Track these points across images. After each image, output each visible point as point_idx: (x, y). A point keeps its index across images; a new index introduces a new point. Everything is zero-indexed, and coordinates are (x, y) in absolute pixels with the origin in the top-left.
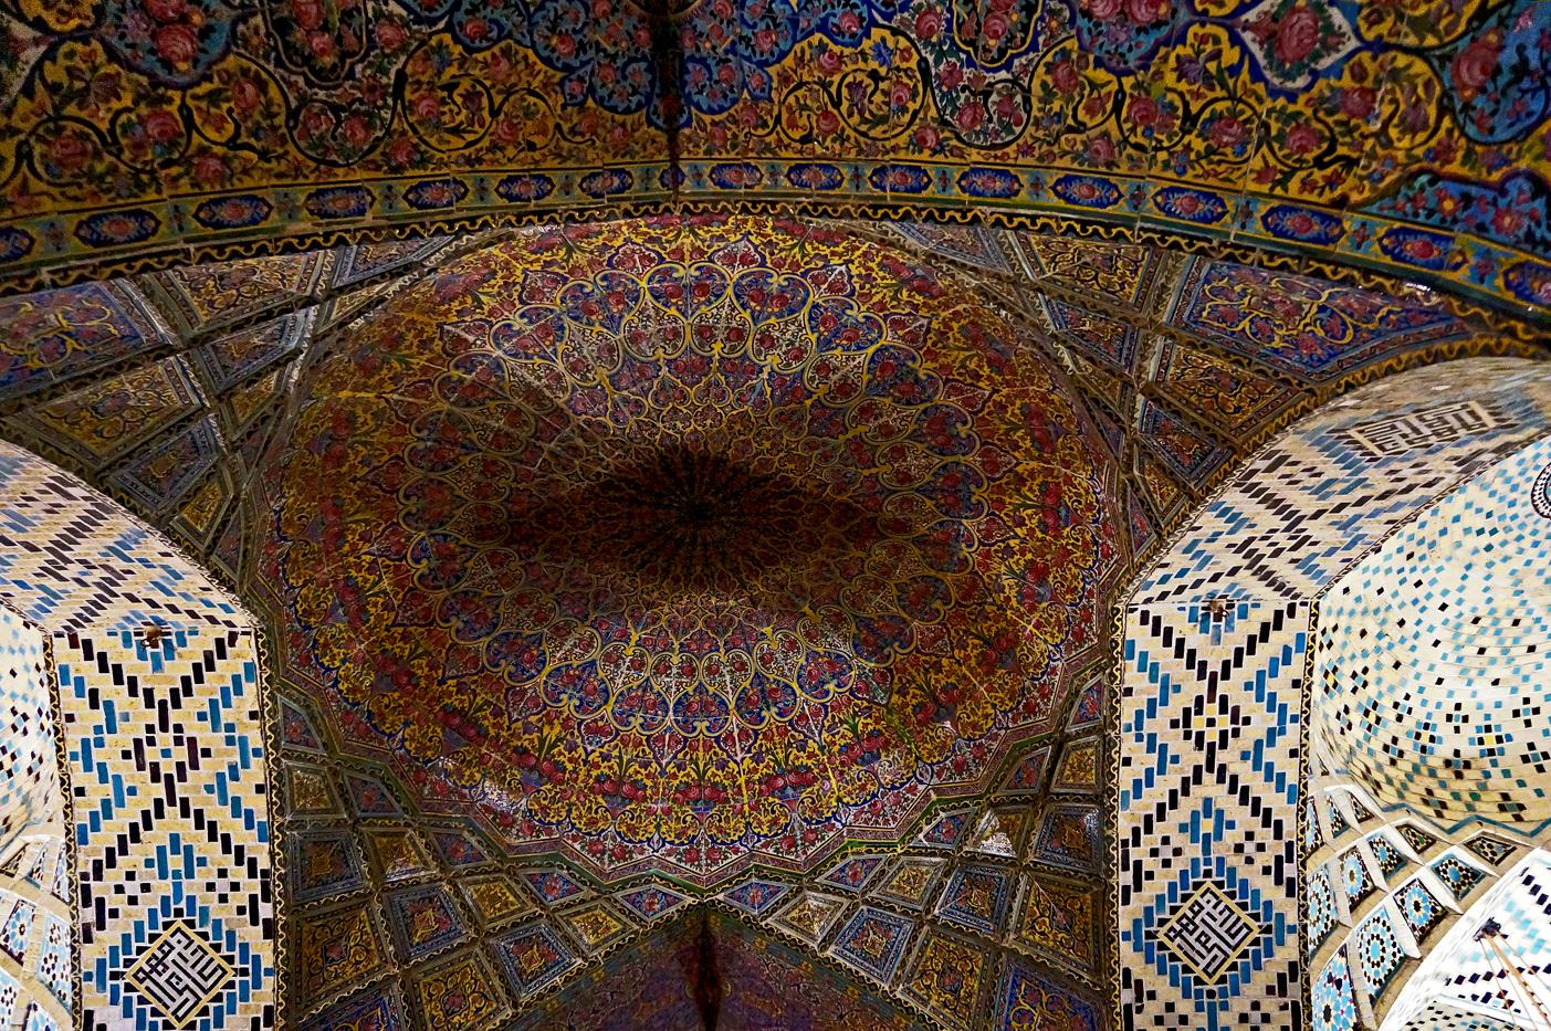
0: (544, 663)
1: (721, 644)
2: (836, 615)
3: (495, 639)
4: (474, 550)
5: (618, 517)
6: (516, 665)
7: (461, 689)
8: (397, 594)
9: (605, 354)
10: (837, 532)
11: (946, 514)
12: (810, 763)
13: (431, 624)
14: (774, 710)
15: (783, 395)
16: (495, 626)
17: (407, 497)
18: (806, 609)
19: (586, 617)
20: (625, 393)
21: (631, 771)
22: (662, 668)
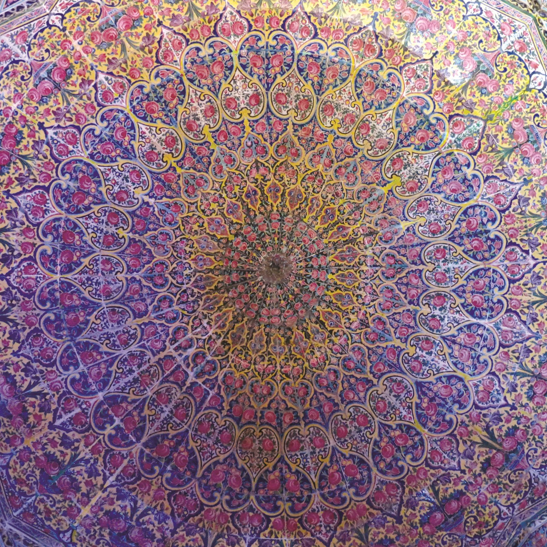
0: (409, 428)
1: (414, 267)
2: (394, 163)
3: (376, 464)
4: (282, 460)
5: (268, 335)
6: (407, 453)
7: (411, 504)
8: (300, 533)
9: (116, 318)
10: (305, 157)
11: (290, 66)
12: (539, 194)
13: (341, 514)
14: (489, 226)
15: (170, 188)
16: (362, 461)
17: (212, 499)
18: (385, 190)
19: (368, 381)
20: (150, 308)
21: (530, 366)
22: (434, 323)
